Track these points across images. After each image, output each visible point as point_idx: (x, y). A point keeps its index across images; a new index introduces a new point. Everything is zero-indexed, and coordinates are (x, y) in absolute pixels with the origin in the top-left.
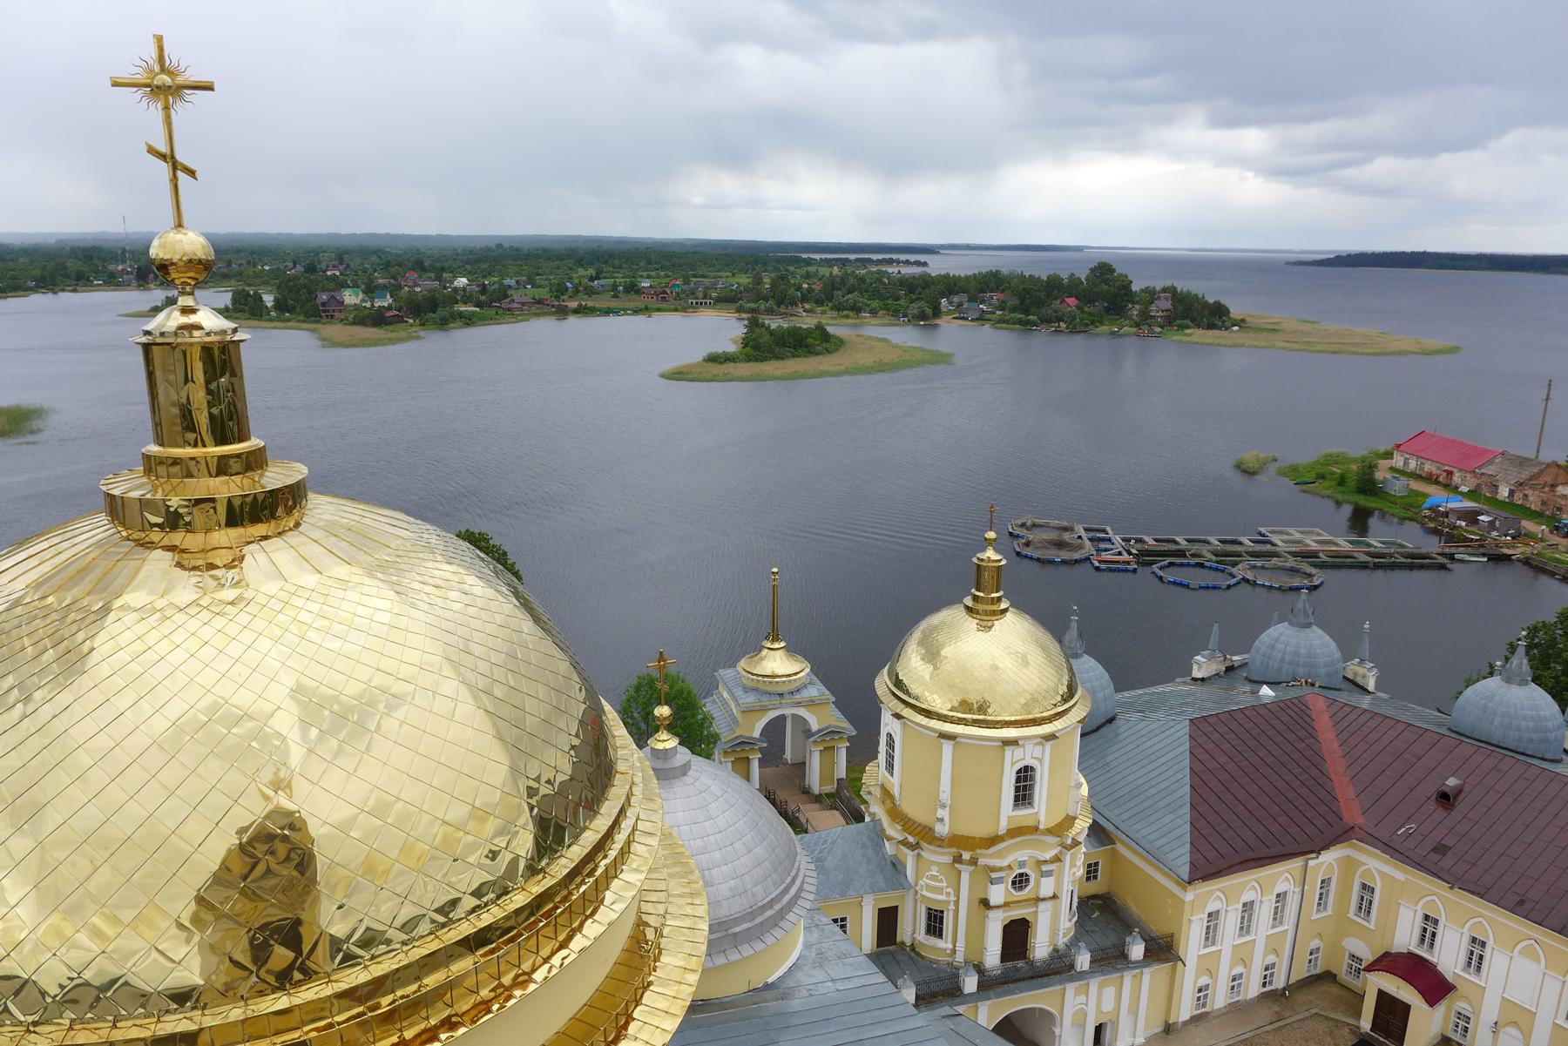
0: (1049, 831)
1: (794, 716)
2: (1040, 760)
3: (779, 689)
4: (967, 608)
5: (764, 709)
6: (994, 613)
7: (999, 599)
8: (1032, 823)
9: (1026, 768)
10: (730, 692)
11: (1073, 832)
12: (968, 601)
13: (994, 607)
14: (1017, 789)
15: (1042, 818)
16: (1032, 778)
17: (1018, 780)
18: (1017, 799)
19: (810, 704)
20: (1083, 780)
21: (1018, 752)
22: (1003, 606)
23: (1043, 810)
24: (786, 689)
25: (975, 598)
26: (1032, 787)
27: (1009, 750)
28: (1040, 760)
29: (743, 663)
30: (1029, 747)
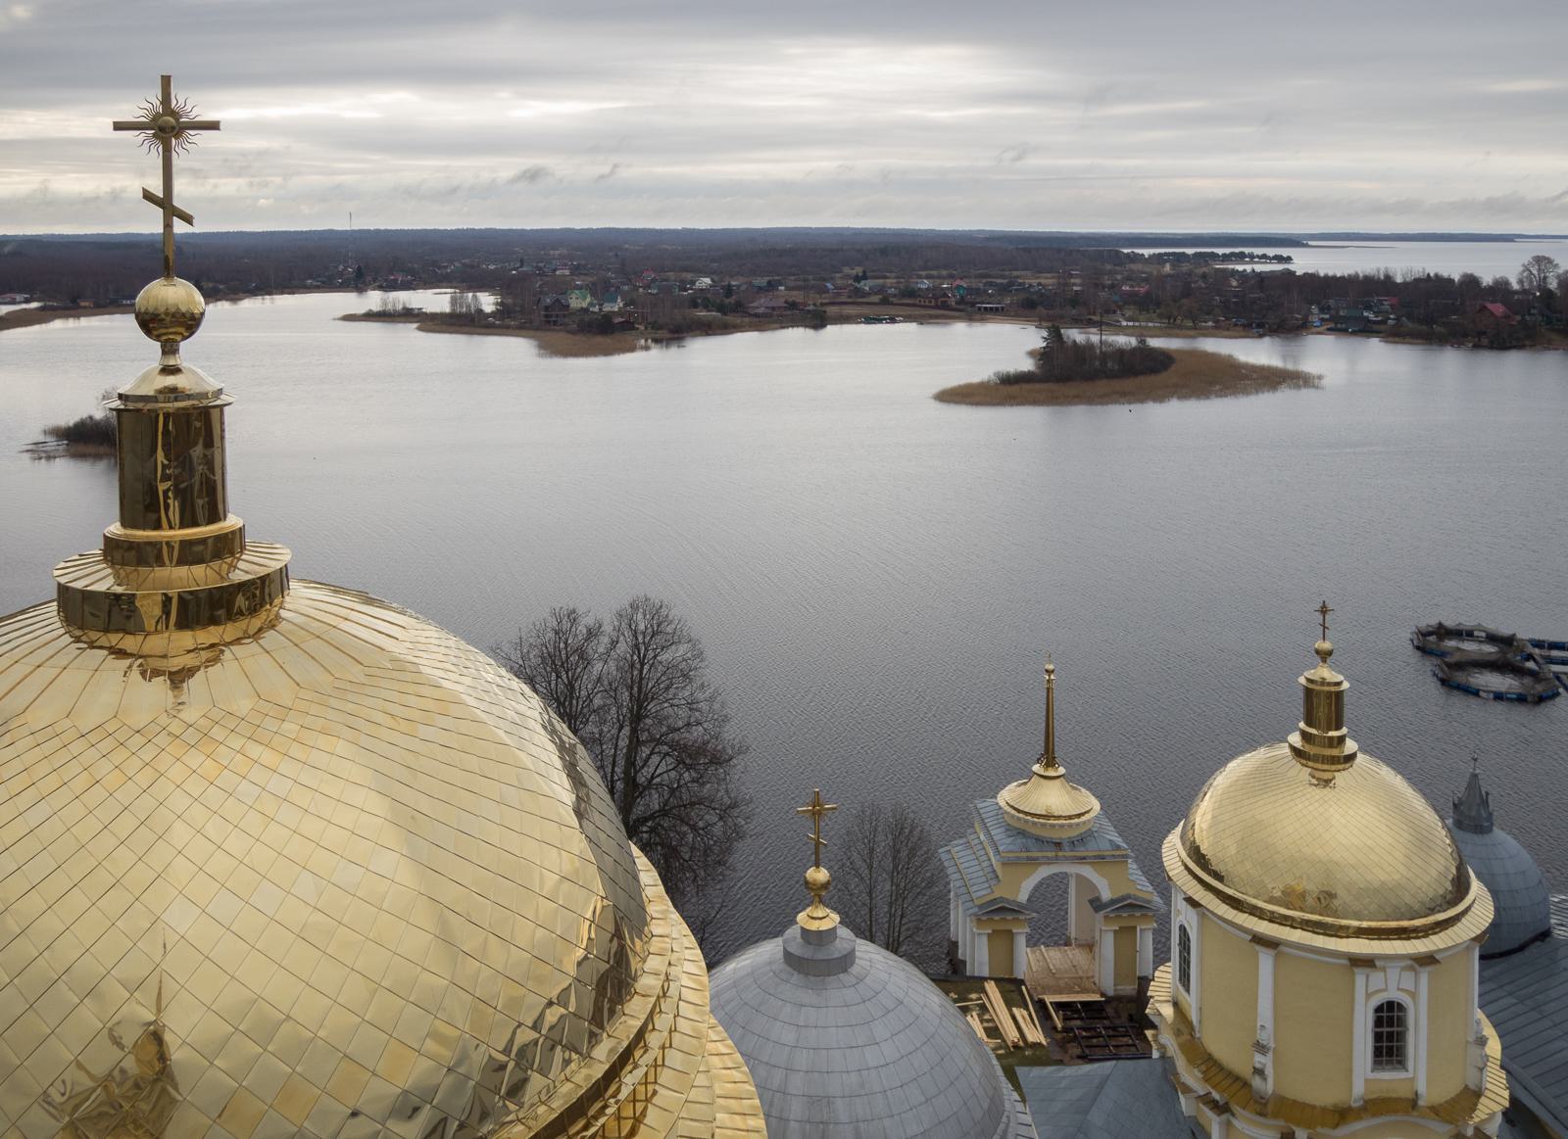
0: (1435, 1110)
1: (1078, 875)
2: (1413, 995)
3: (1056, 835)
4: (1294, 749)
5: (1033, 862)
6: (1334, 760)
7: (1341, 740)
8: (1404, 1092)
9: (1391, 1005)
10: (988, 832)
11: (1480, 1114)
12: (1295, 739)
13: (1335, 752)
14: (1378, 1037)
15: (1422, 1087)
16: (1401, 1022)
17: (1378, 1022)
18: (1378, 1052)
19: (1099, 860)
20: (1489, 1031)
21: (1377, 978)
22: (1350, 746)
23: (1423, 1072)
24: (1065, 835)
25: (1305, 736)
26: (1401, 1037)
27: (1360, 977)
28: (1413, 995)
29: (1007, 795)
30: (1393, 974)
